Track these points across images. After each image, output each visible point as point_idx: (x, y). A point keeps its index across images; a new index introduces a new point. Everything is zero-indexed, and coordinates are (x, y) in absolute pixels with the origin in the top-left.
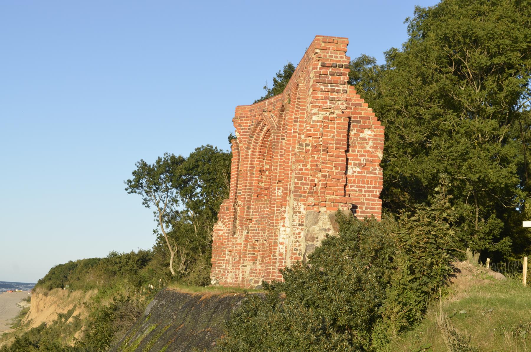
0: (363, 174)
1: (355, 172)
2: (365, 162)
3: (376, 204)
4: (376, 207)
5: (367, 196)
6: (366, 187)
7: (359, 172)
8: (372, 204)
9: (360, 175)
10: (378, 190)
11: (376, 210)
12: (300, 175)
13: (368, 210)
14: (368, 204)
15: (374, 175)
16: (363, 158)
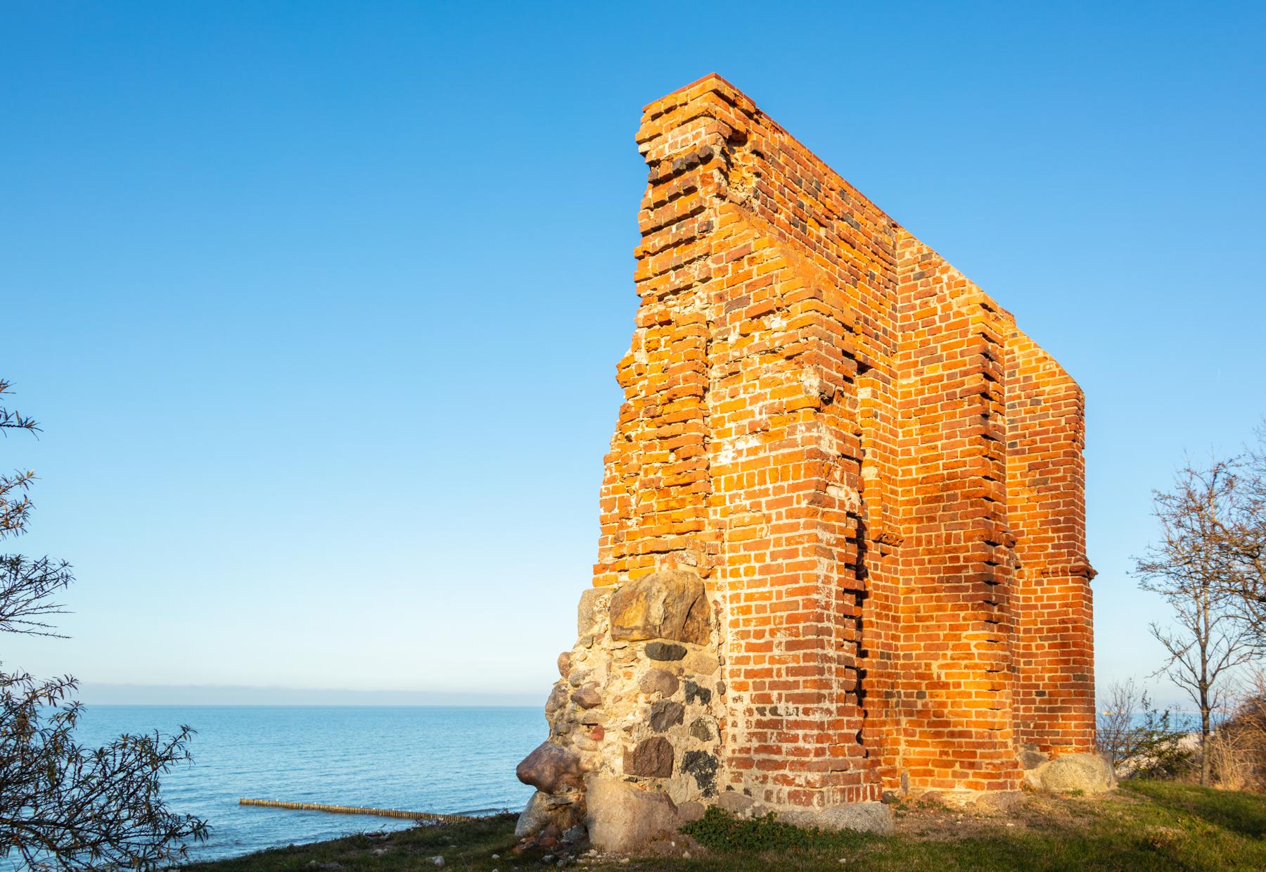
0: (762, 454)
1: (740, 452)
2: (764, 416)
3: (800, 536)
4: (800, 547)
5: (774, 517)
6: (771, 492)
7: (753, 451)
8: (789, 541)
9: (752, 458)
10: (801, 493)
11: (801, 558)
12: (611, 496)
13: (780, 561)
14: (777, 542)
15: (791, 450)
16: (761, 404)
